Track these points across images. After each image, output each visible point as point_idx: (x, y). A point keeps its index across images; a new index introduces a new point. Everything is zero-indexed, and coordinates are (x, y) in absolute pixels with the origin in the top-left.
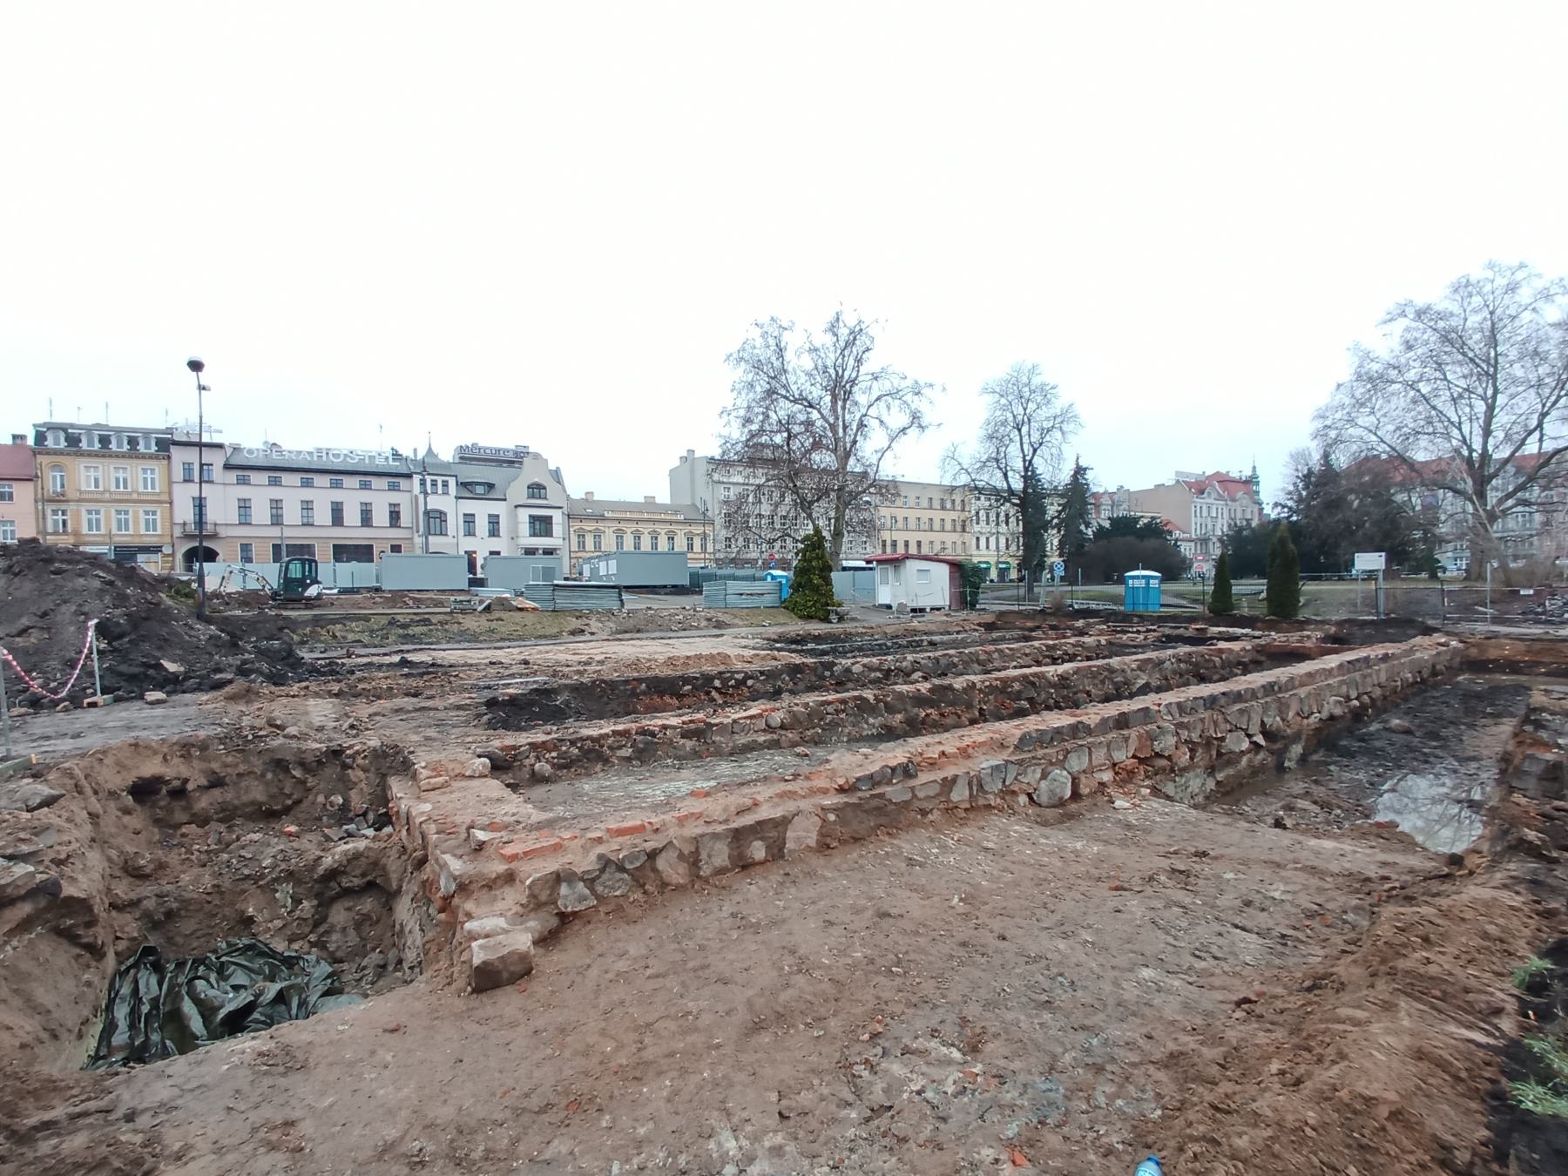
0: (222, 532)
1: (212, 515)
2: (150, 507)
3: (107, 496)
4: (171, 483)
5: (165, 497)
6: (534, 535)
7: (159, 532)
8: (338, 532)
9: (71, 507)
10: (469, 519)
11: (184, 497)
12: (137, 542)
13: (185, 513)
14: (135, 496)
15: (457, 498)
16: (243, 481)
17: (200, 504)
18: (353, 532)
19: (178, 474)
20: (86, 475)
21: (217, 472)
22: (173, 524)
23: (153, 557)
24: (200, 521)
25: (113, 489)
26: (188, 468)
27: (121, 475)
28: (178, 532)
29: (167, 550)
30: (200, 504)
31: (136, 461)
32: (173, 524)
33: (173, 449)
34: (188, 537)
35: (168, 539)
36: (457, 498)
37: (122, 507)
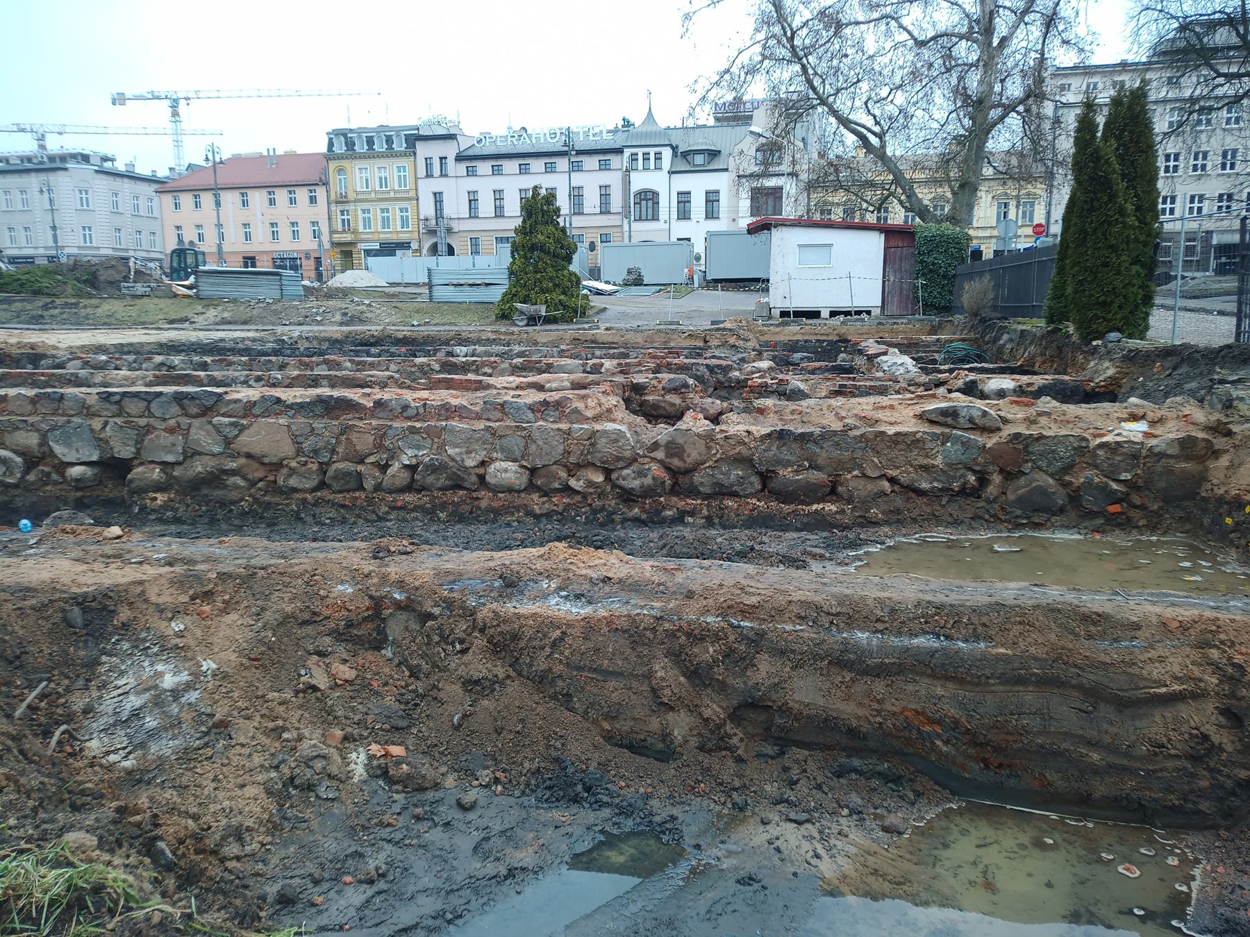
0: (456, 226)
1: (448, 211)
2: (404, 204)
3: (373, 195)
4: (416, 179)
5: (412, 194)
9: (351, 207)
10: (684, 199)
12: (394, 238)
13: (427, 209)
14: (392, 195)
15: (671, 173)
17: (438, 197)
19: (422, 172)
20: (361, 176)
25: (378, 188)
27: (383, 175)
29: (414, 246)
30: (438, 197)
31: (392, 160)
32: (418, 219)
33: (419, 145)
35: (416, 235)
36: (671, 173)
37: (384, 205)
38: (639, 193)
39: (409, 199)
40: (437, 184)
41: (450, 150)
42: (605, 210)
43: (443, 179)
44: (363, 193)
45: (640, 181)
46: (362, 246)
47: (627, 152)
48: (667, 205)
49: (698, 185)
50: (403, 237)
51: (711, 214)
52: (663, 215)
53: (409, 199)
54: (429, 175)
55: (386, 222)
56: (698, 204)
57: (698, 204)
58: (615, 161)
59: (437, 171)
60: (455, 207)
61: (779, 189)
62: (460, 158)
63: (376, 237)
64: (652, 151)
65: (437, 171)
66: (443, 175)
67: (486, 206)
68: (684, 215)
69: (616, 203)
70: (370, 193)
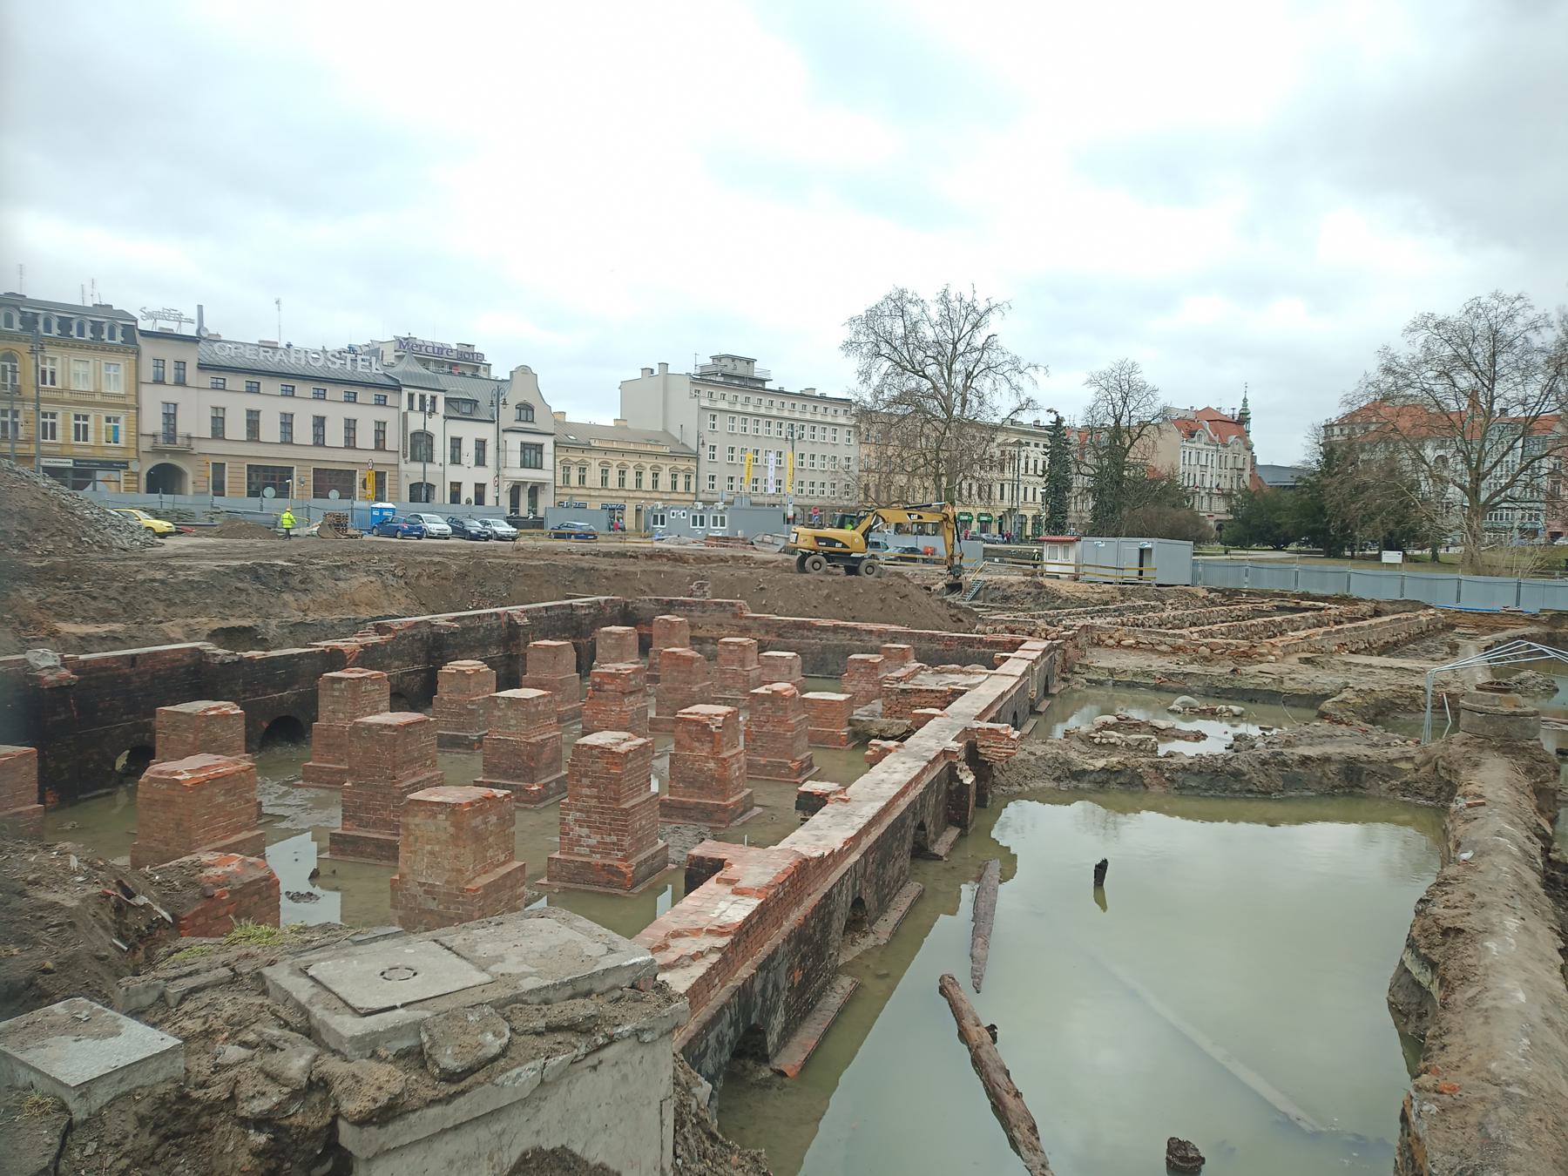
0: (199, 448)
2: (112, 413)
4: (138, 383)
5: (130, 401)
6: (523, 465)
7: (122, 443)
8: (319, 453)
11: (153, 402)
12: (100, 455)
13: (153, 422)
16: (219, 387)
18: (335, 455)
19: (148, 373)
21: (191, 374)
22: (139, 435)
23: (114, 475)
24: (170, 434)
26: (159, 363)
28: (146, 444)
29: (134, 467)
34: (156, 451)
35: (133, 454)
38: (413, 435)
39: (126, 407)
40: (172, 394)
41: (192, 357)
42: (380, 445)
43: (179, 389)
44: (48, 390)
45: (416, 422)
46: (45, 462)
47: (405, 392)
48: (441, 449)
49: (469, 433)
50: (114, 455)
51: (480, 461)
52: (438, 458)
53: (126, 407)
54: (159, 381)
55: (81, 432)
56: (468, 449)
57: (468, 449)
58: (391, 398)
59: (170, 376)
60: (195, 422)
61: (541, 446)
62: (202, 367)
63: (67, 451)
64: (428, 395)
65: (170, 376)
66: (181, 382)
67: (236, 427)
68: (456, 460)
69: (393, 440)
70: (61, 391)
